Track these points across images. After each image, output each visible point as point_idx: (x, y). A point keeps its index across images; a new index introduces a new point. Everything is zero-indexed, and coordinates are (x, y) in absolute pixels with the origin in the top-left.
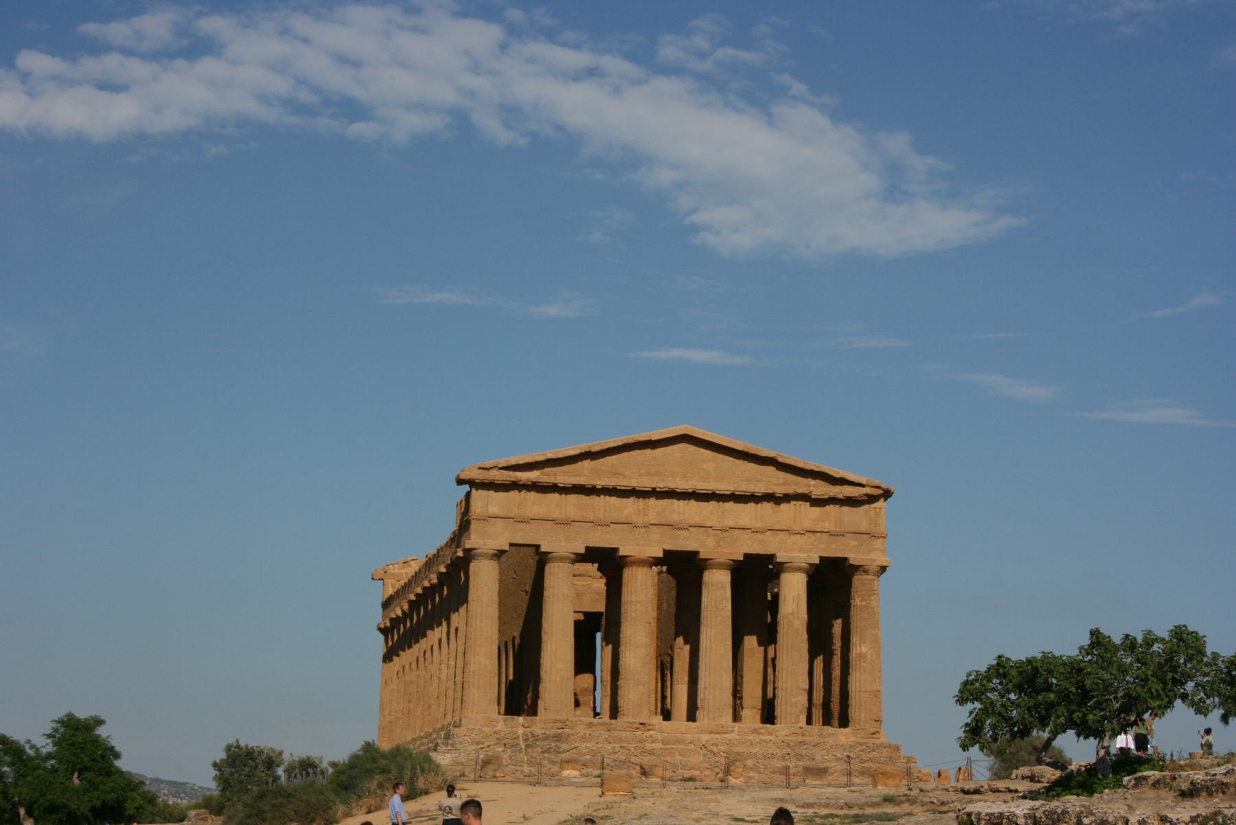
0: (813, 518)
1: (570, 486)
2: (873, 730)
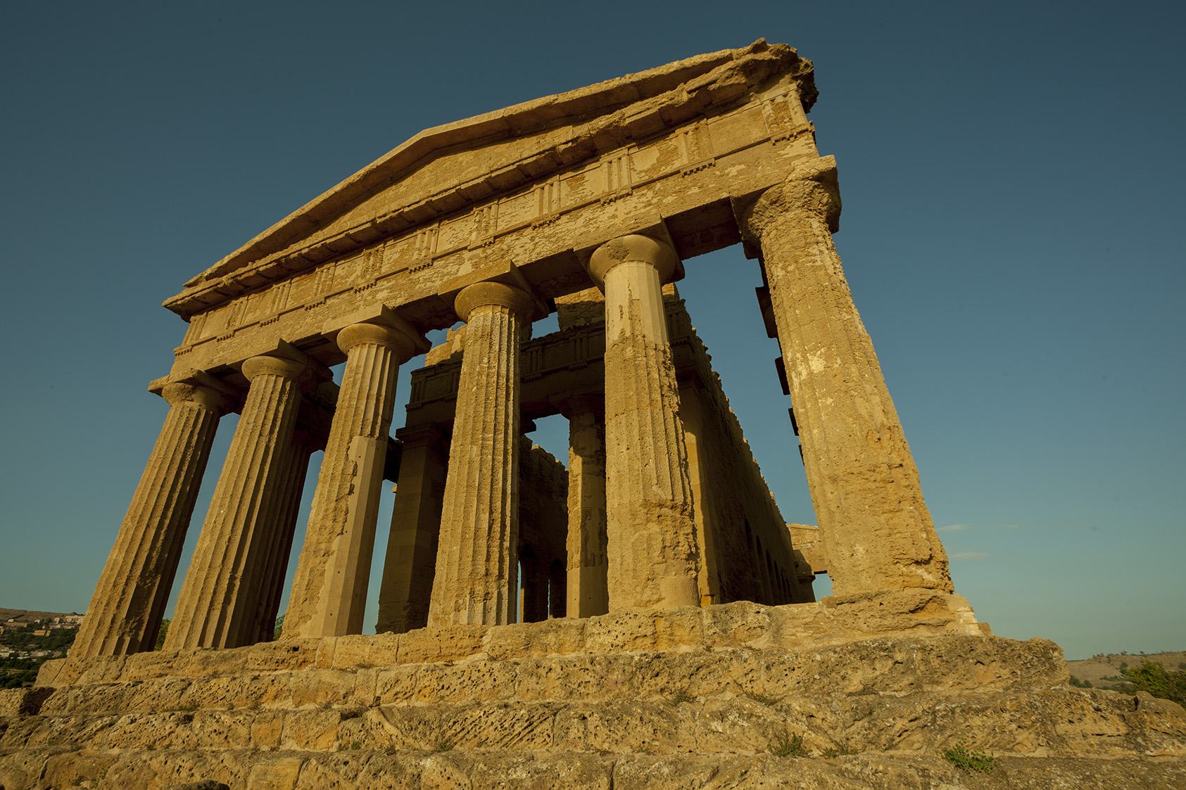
0: (645, 168)
1: (271, 265)
2: (913, 595)
